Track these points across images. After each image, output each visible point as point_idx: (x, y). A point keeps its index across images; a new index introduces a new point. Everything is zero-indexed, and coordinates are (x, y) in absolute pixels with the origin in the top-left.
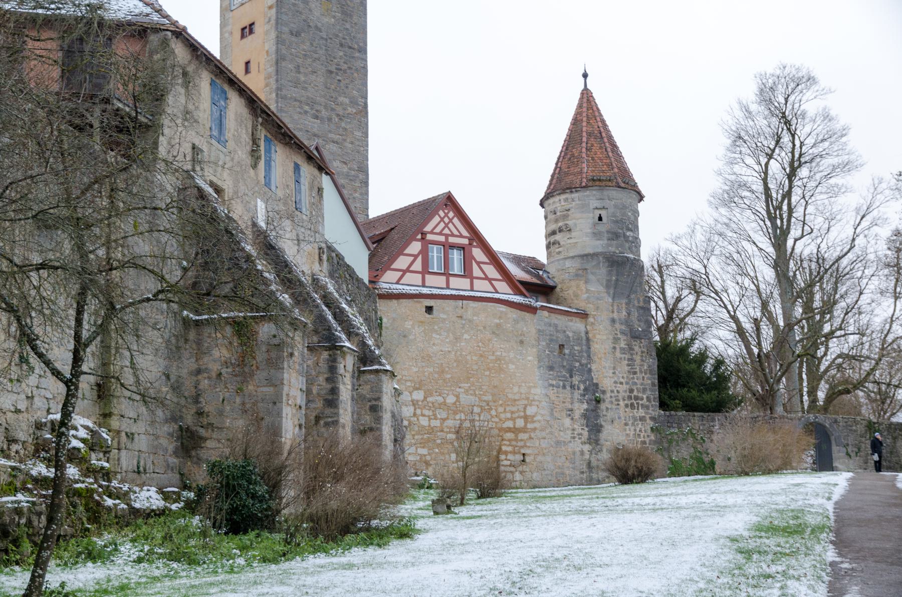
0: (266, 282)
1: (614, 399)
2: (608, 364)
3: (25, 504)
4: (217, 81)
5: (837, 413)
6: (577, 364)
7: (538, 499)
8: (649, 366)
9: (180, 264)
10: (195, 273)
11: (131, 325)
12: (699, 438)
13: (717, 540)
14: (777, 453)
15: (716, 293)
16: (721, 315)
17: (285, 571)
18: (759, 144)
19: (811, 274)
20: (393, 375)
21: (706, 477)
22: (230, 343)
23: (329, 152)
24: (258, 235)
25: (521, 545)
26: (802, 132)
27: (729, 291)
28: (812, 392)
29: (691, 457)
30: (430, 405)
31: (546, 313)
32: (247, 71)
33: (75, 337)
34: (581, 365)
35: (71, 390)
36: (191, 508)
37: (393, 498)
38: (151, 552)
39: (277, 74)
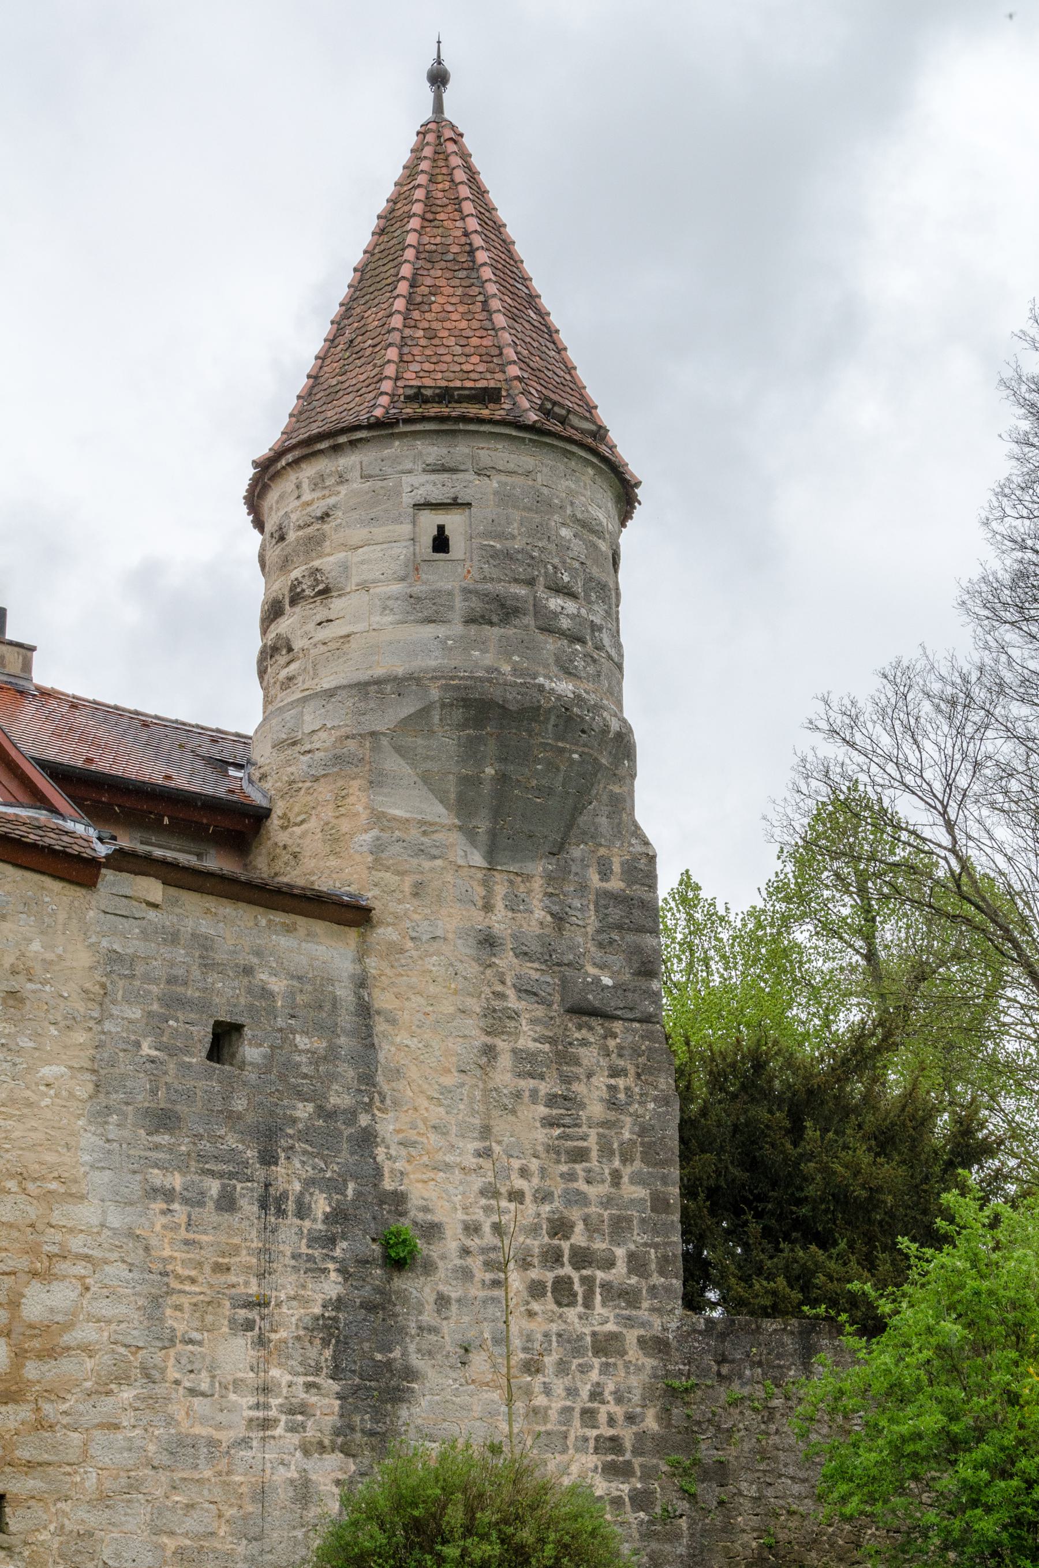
1: (475, 1263)
6: (303, 1111)
34: (322, 1112)
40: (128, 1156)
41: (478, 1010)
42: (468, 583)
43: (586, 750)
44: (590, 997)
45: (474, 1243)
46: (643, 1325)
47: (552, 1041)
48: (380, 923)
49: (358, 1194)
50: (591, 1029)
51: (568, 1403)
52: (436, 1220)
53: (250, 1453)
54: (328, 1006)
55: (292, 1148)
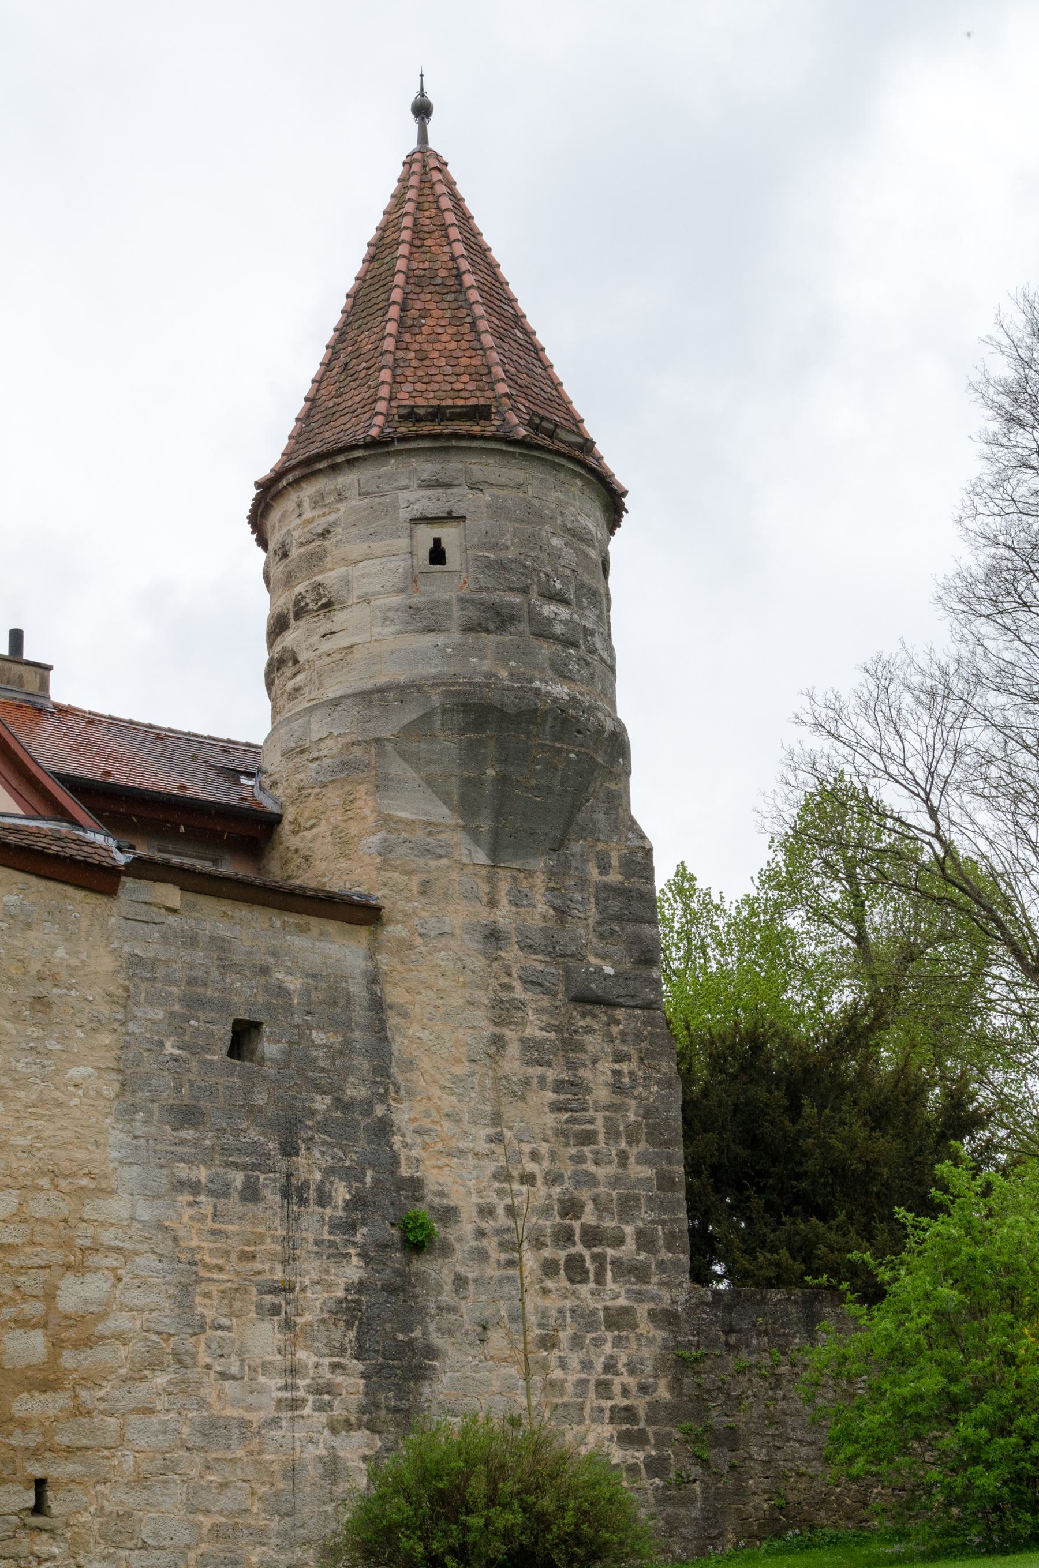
1: (491, 1244)
6: (322, 1103)
34: (340, 1104)
40: (155, 1152)
41: (486, 1002)
42: (465, 593)
43: (583, 750)
44: (593, 986)
45: (488, 1225)
46: (653, 1299)
47: (558, 1029)
48: (390, 921)
49: (377, 1181)
50: (595, 1016)
51: (583, 1376)
52: (452, 1204)
53: (280, 1433)
54: (342, 1002)
55: (312, 1139)
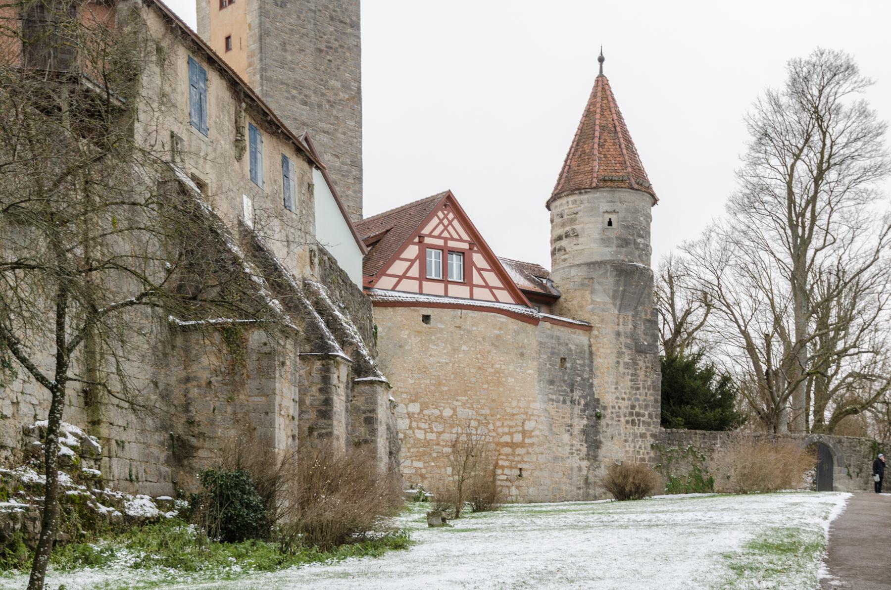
0: (255, 287)
1: (614, 416)
2: (610, 378)
3: (19, 510)
4: (195, 59)
5: (842, 433)
6: (579, 379)
7: (533, 514)
8: (653, 382)
9: (163, 265)
10: (179, 275)
11: (115, 330)
12: (699, 456)
13: (710, 556)
14: (777, 472)
15: (728, 306)
16: (731, 330)
17: (281, 579)
18: (786, 143)
19: (829, 287)
20: (388, 386)
21: (704, 495)
22: (219, 350)
23: (320, 143)
24: (245, 236)
25: (514, 557)
26: (835, 129)
27: (742, 305)
28: (819, 412)
29: (690, 475)
30: (426, 418)
31: (548, 325)
32: (228, 48)
33: (57, 342)
34: (583, 379)
35: (57, 397)
36: (185, 516)
37: (387, 510)
38: (147, 558)
39: (261, 53)
45: (614, 411)
